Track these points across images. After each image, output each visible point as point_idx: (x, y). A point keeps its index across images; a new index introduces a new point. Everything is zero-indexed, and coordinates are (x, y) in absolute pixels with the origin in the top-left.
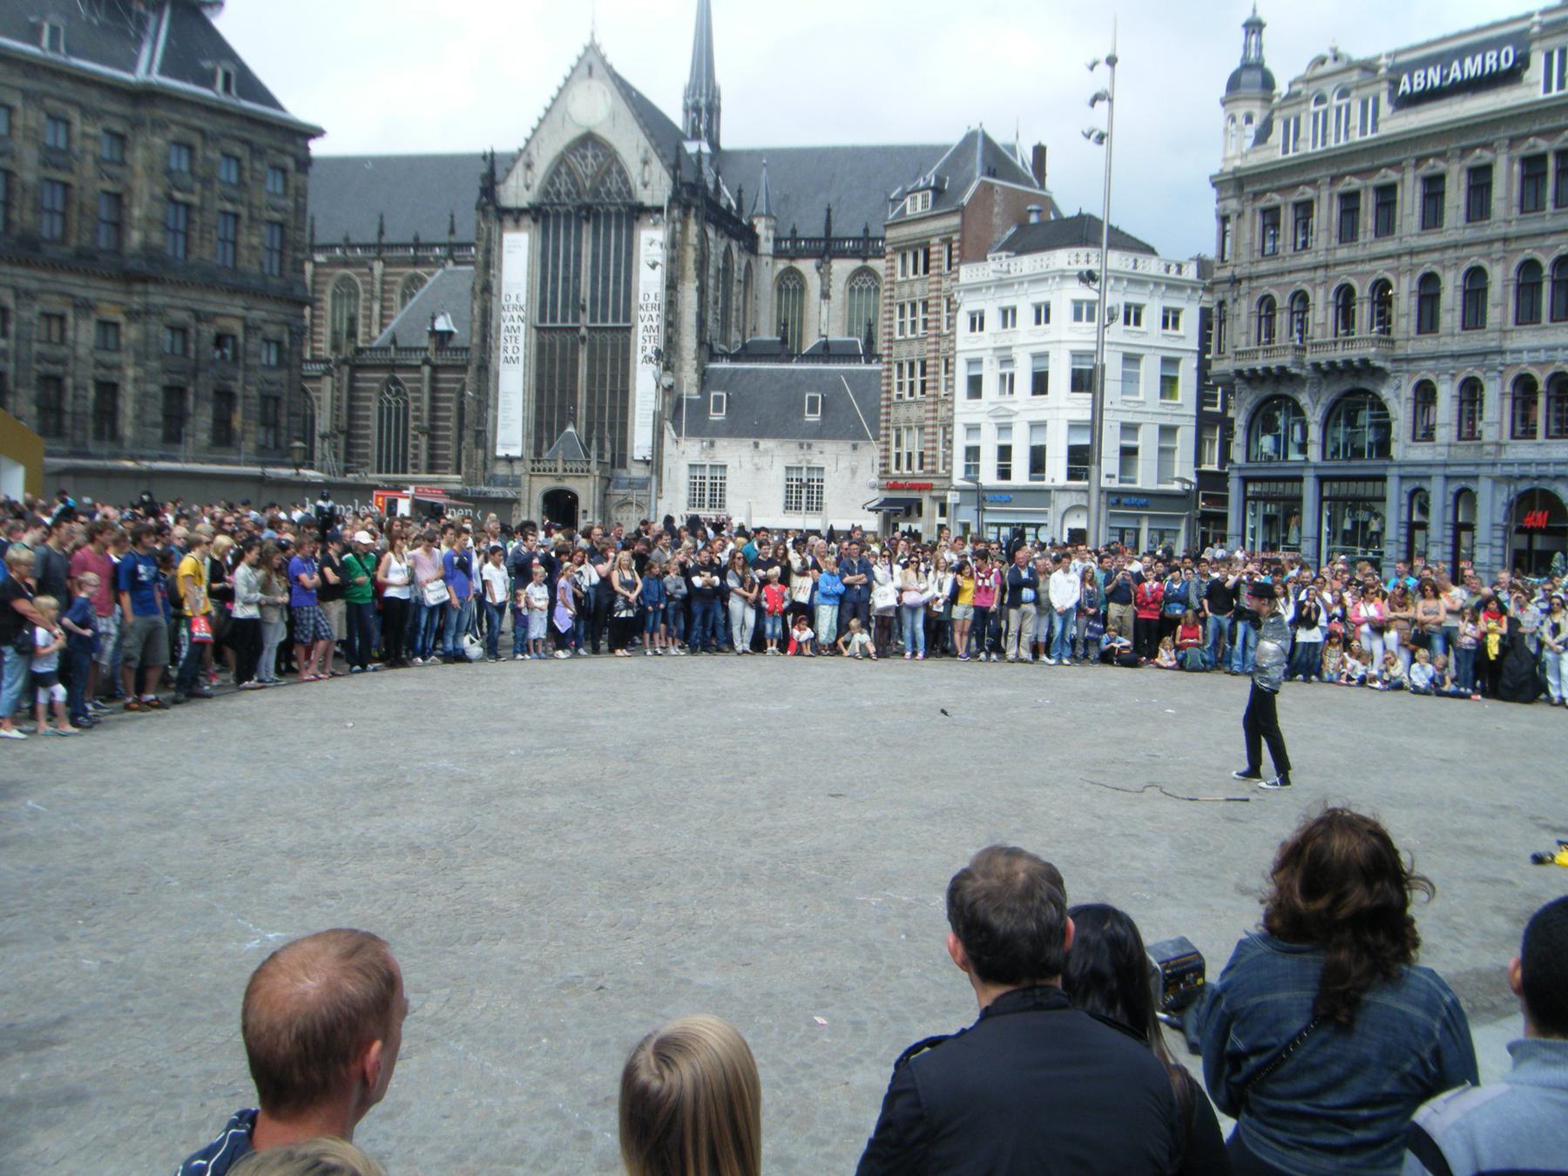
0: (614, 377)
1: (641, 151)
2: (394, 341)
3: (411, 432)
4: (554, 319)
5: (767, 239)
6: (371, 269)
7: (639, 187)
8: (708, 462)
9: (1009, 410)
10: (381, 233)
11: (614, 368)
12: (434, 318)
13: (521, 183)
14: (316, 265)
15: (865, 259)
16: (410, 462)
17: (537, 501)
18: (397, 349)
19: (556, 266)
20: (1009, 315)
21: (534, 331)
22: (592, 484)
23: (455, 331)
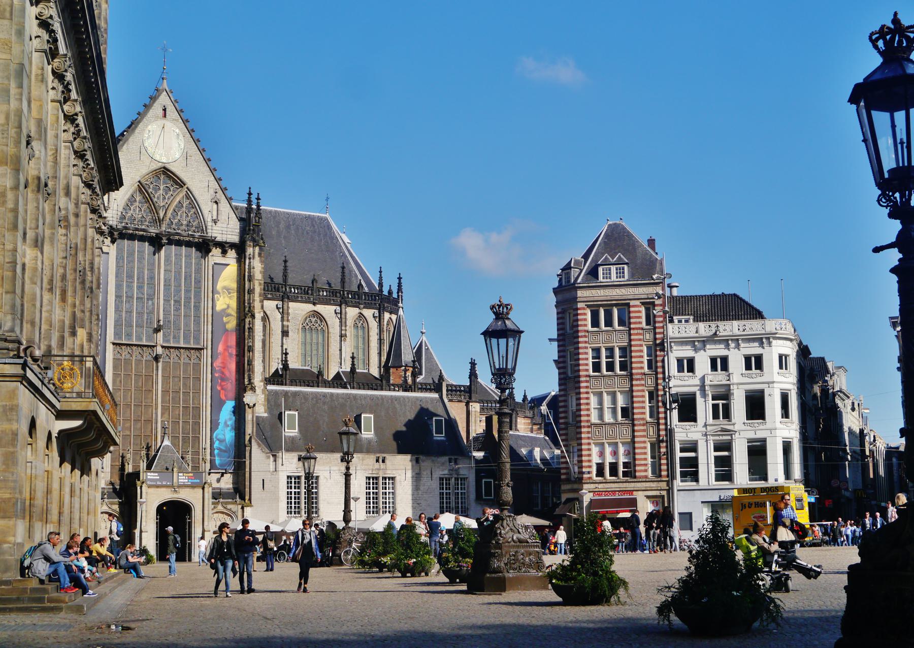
0: (186, 394)
1: (212, 191)
4: (129, 335)
7: (210, 224)
9: (729, 431)
19: (130, 287)
20: (720, 364)
21: (112, 345)
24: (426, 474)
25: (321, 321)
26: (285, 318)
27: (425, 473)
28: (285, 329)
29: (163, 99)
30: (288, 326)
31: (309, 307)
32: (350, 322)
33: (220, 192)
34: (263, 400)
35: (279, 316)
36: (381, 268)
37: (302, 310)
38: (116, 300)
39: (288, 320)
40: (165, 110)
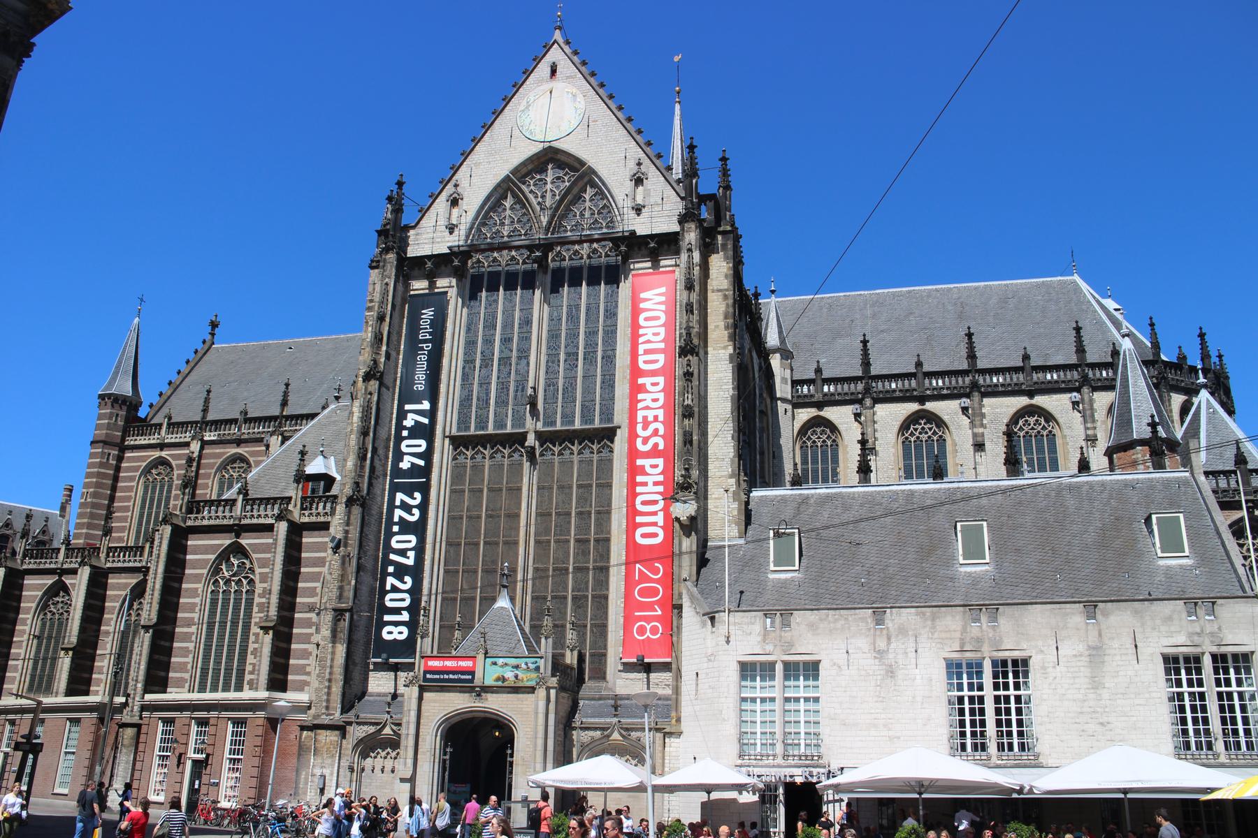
2: (244, 491)
3: (255, 629)
5: (784, 380)
6: (268, 446)
8: (778, 657)
10: (284, 403)
11: (583, 500)
12: (303, 453)
13: (443, 222)
14: (204, 444)
15: (922, 400)
16: (247, 677)
17: (431, 740)
18: (246, 501)
19: (489, 342)
21: (447, 441)
22: (542, 705)
23: (338, 478)
24: (1118, 646)
25: (1047, 421)
26: (977, 423)
27: (1116, 644)
28: (979, 439)
29: (555, 55)
30: (983, 435)
31: (1023, 401)
32: (1100, 414)
33: (646, 161)
34: (735, 513)
35: (966, 421)
36: (1151, 318)
37: (1008, 406)
38: (464, 368)
39: (982, 425)
40: (554, 71)
